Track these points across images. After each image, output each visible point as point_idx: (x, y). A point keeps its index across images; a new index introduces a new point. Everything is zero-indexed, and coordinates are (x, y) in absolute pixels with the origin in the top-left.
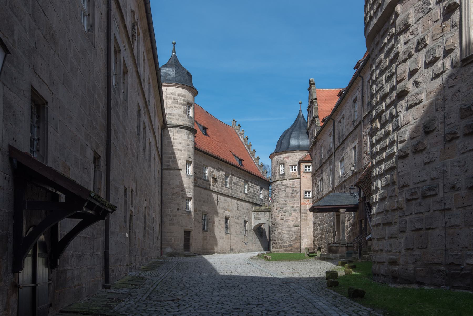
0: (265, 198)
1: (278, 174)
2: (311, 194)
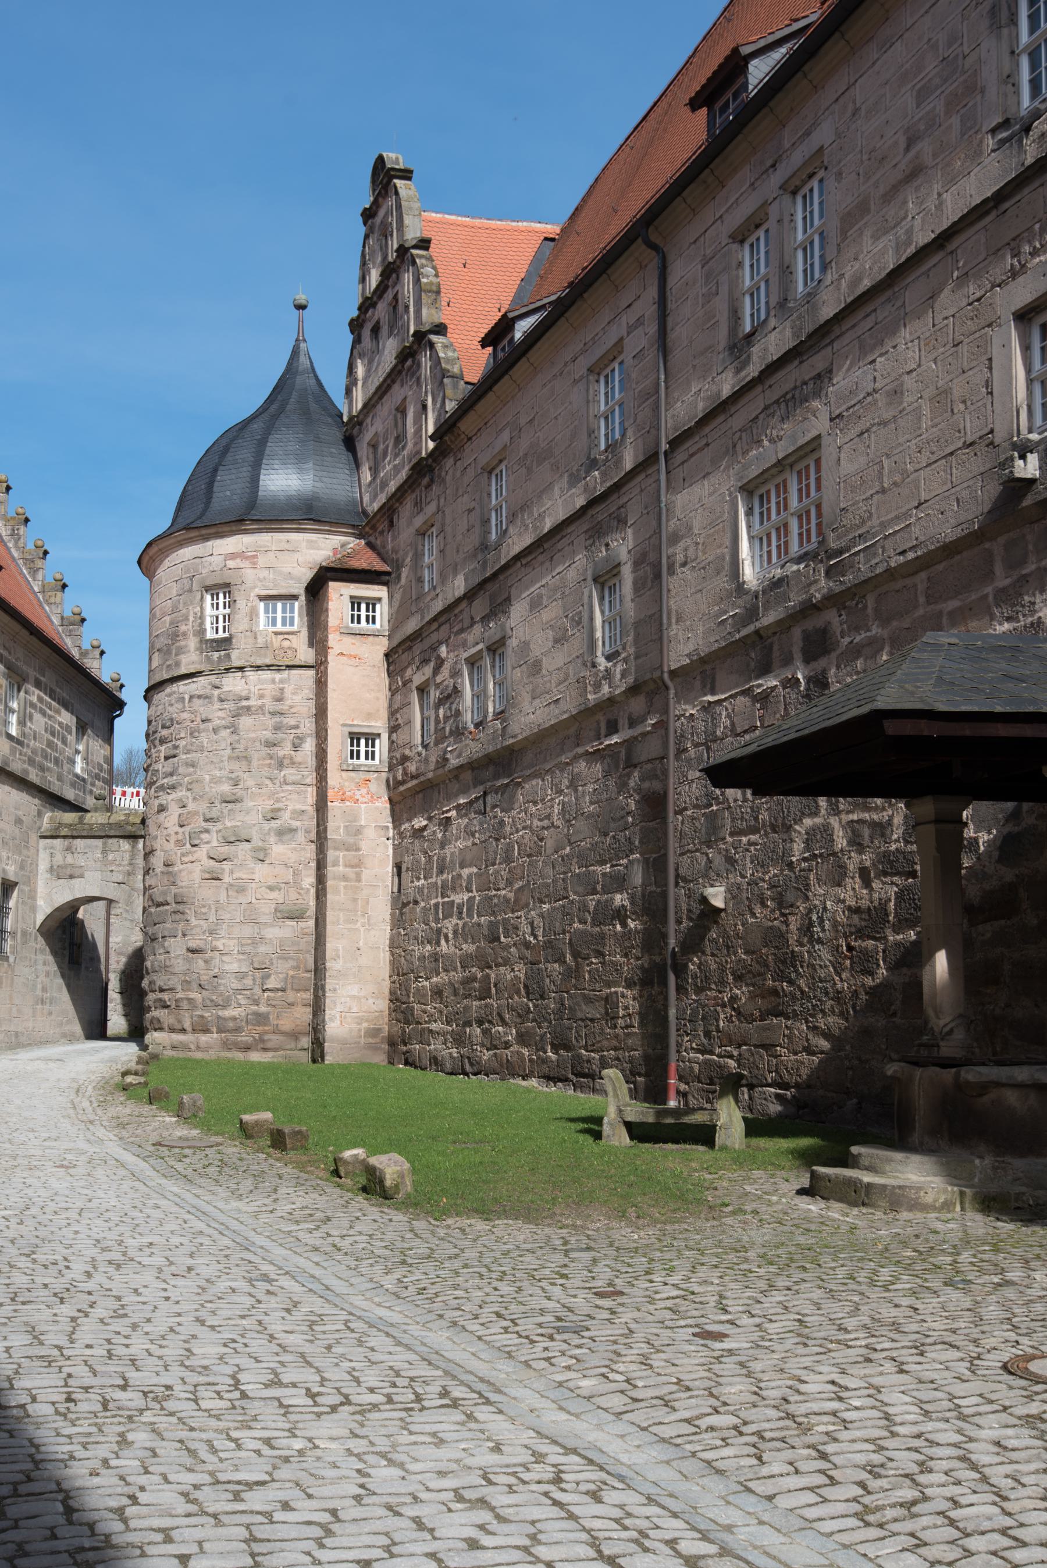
0: (97, 777)
1: (192, 643)
2: (381, 747)
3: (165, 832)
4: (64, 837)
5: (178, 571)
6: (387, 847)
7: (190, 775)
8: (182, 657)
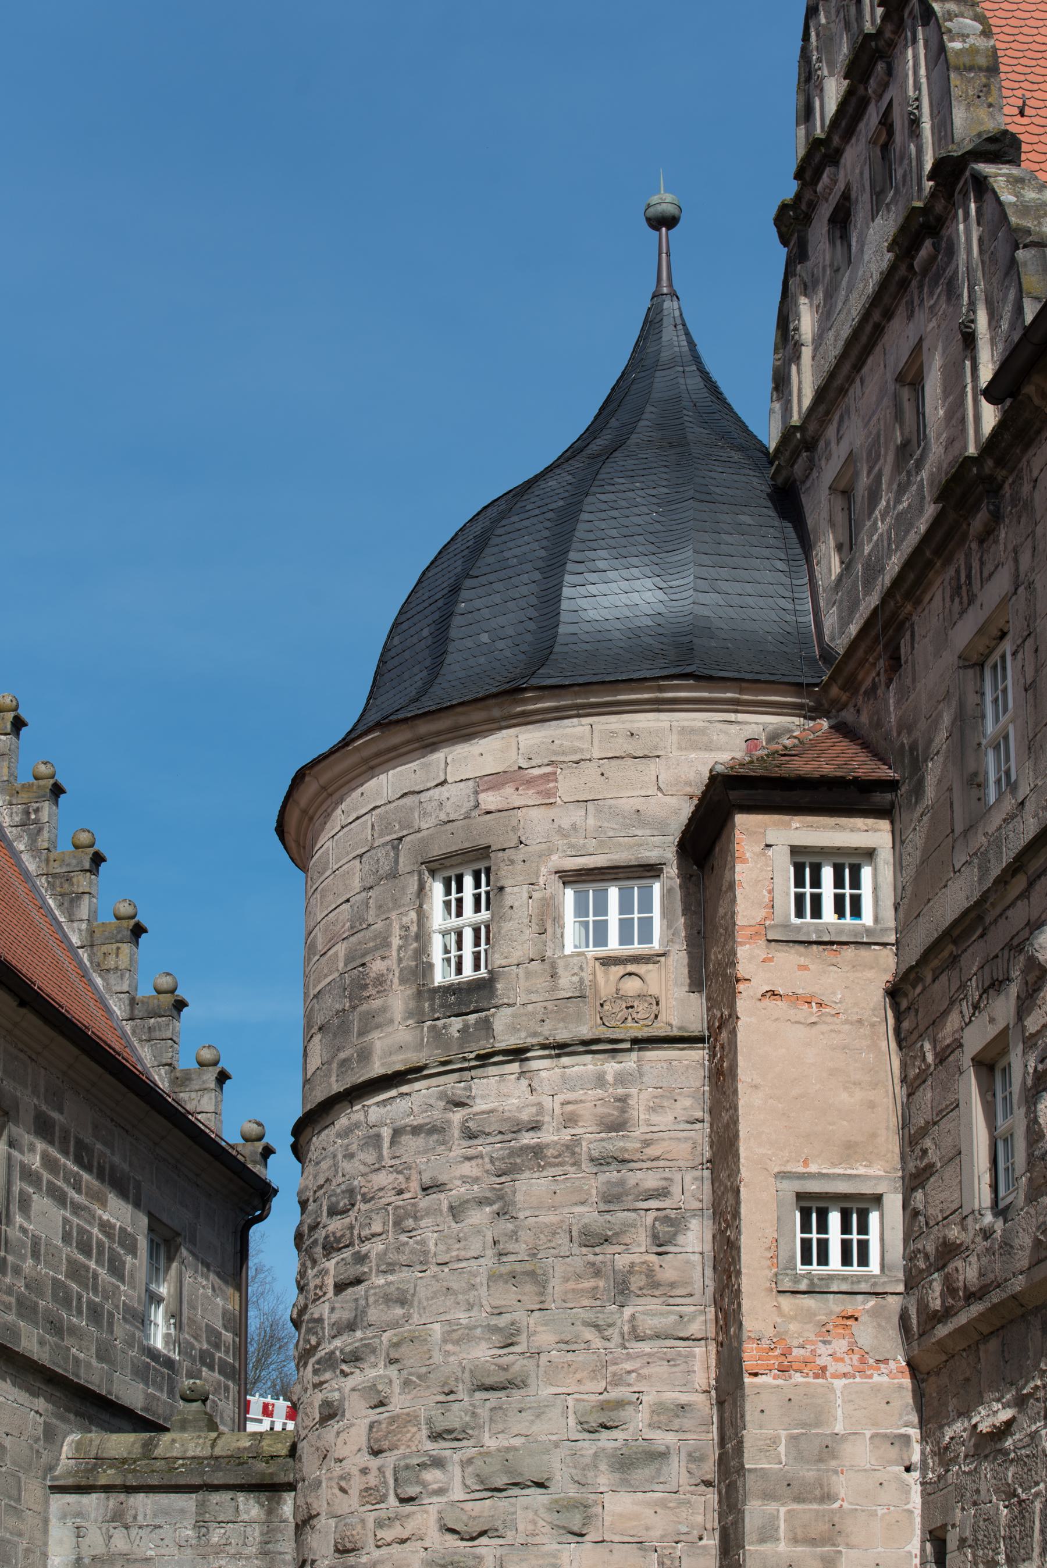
0: (206, 1359)
1: (398, 1000)
2: (884, 1231)
3: (338, 1471)
4: (107, 1489)
5: (363, 831)
6: (905, 1489)
7: (395, 1325)
8: (375, 1035)
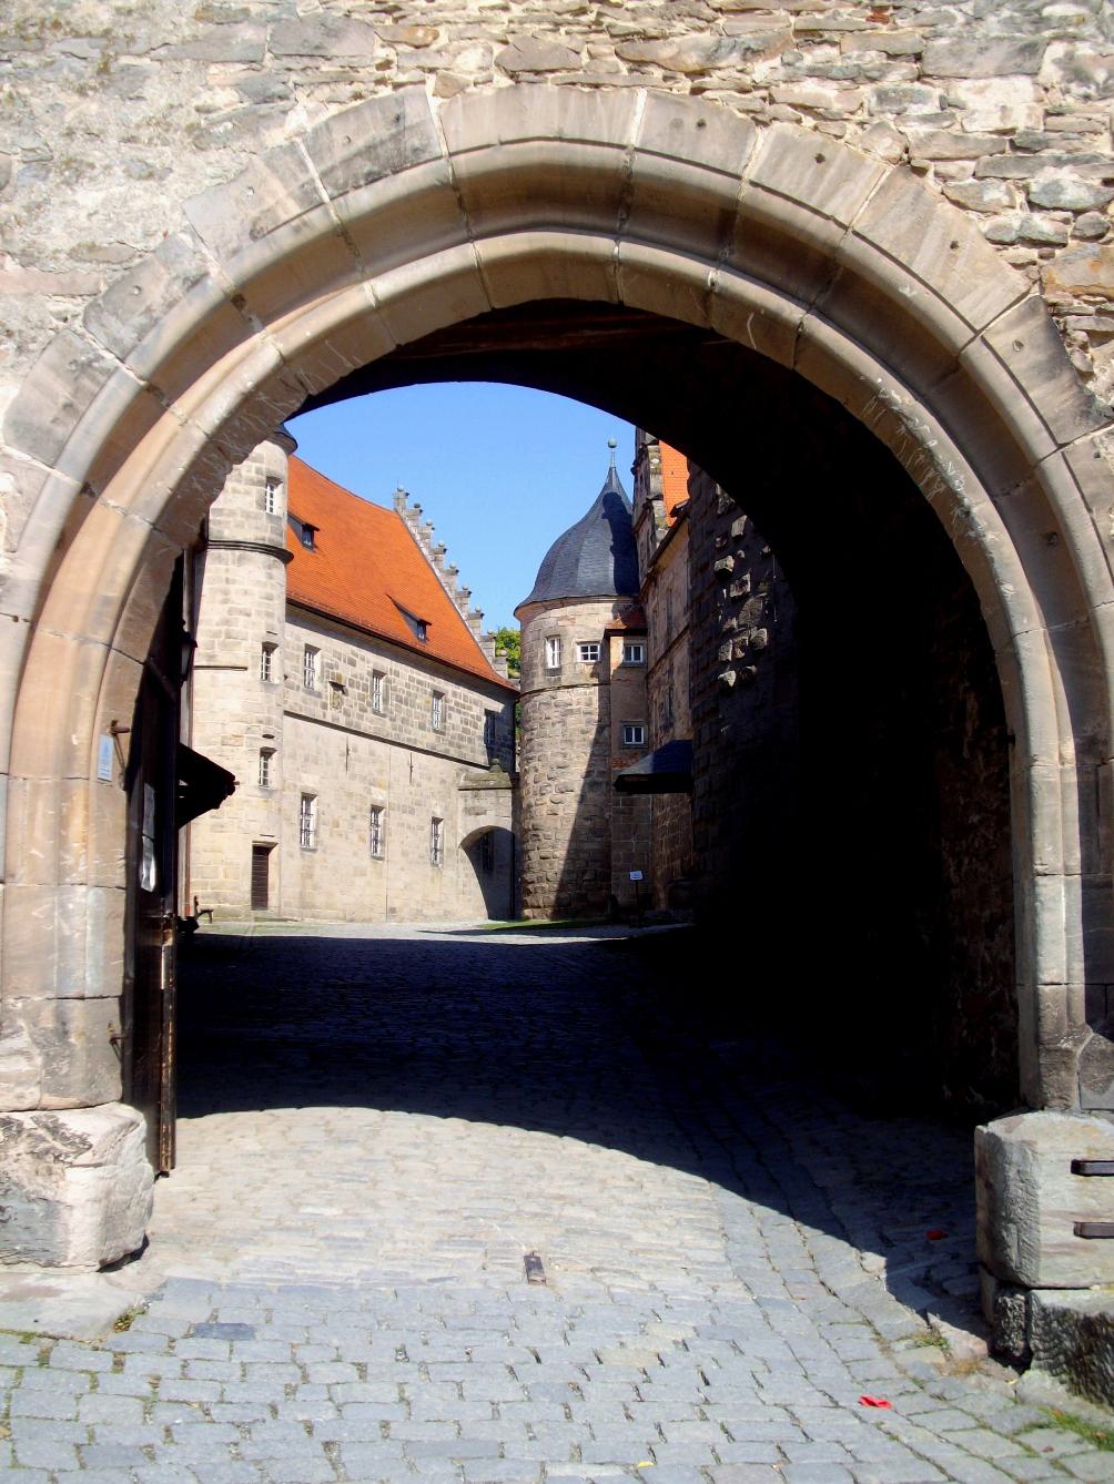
1: (540, 671)
